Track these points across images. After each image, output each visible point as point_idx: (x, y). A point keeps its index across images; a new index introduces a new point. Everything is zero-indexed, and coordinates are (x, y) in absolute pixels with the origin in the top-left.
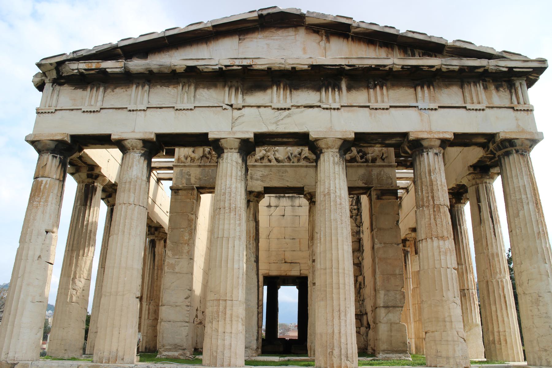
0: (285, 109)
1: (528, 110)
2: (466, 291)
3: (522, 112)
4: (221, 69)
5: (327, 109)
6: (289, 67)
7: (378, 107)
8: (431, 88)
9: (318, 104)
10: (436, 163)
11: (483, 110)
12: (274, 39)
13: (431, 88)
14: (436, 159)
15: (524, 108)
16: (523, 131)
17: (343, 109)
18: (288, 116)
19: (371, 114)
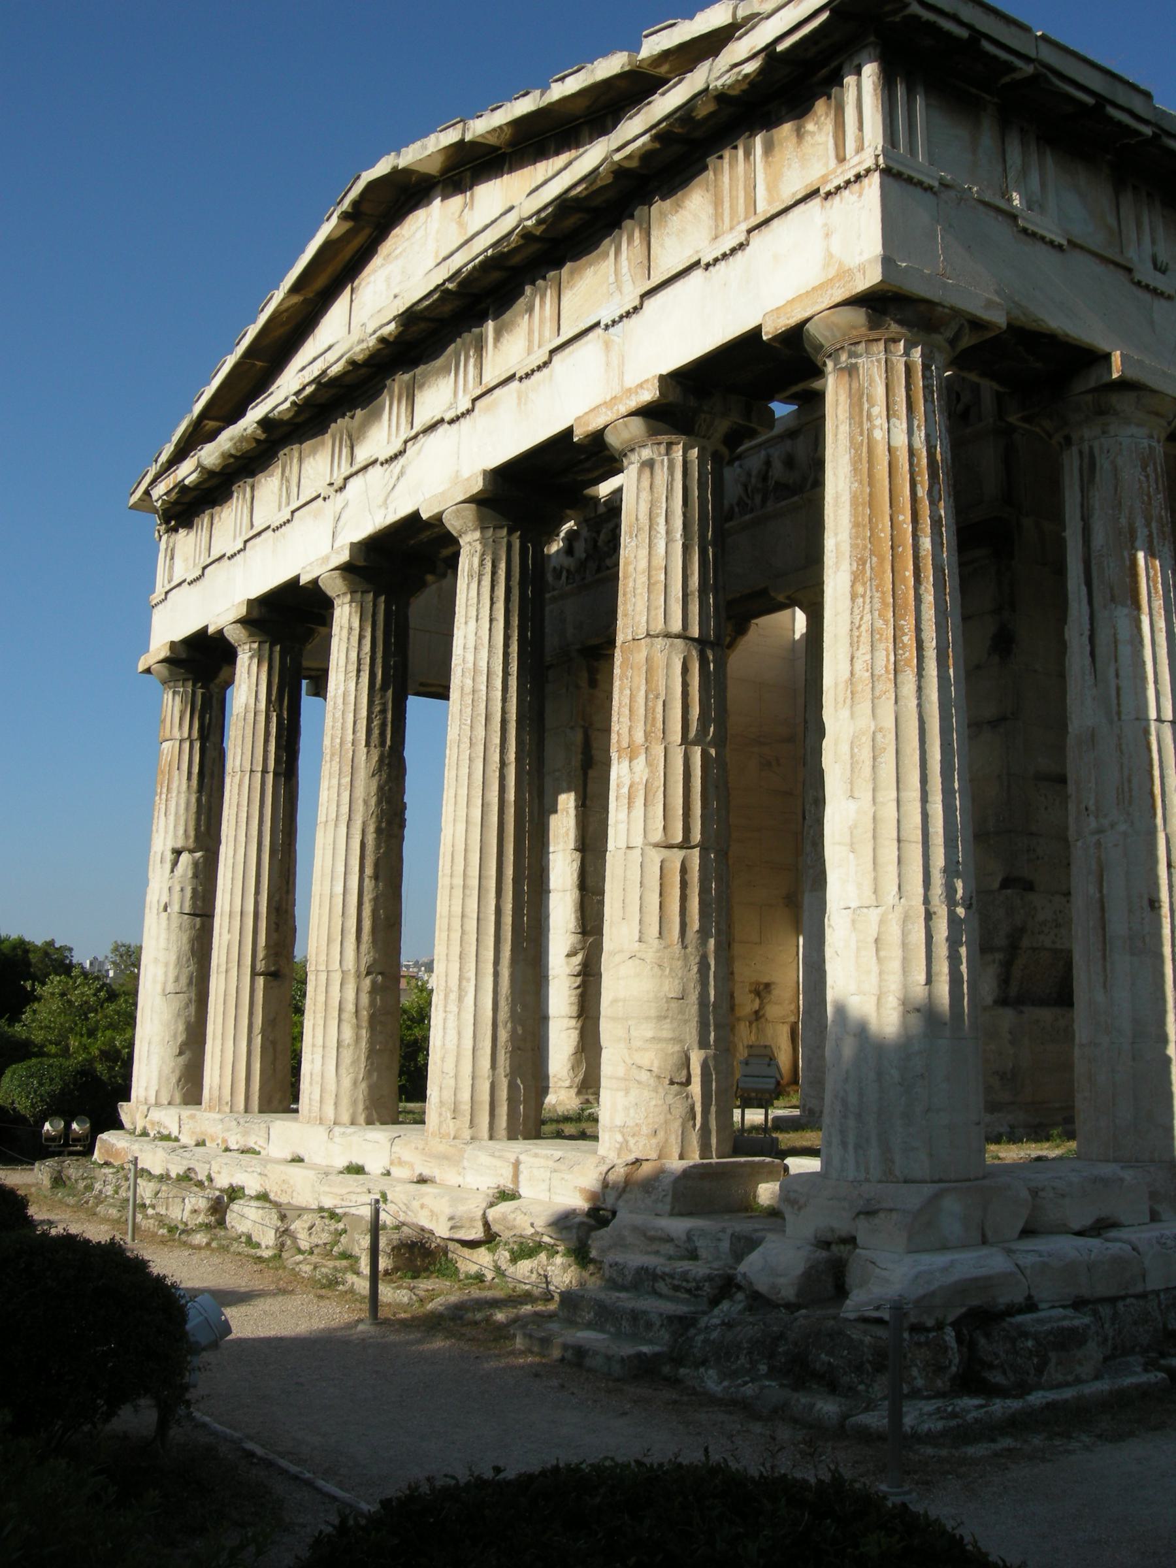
0: (395, 457)
1: (858, 177)
3: (846, 193)
4: (294, 403)
5: (452, 422)
6: (372, 342)
7: (528, 370)
8: (637, 234)
9: (438, 417)
10: (645, 495)
11: (741, 246)
12: (397, 258)
13: (637, 234)
14: (646, 483)
15: (846, 178)
16: (844, 274)
17: (478, 404)
18: (402, 473)
19: (519, 398)
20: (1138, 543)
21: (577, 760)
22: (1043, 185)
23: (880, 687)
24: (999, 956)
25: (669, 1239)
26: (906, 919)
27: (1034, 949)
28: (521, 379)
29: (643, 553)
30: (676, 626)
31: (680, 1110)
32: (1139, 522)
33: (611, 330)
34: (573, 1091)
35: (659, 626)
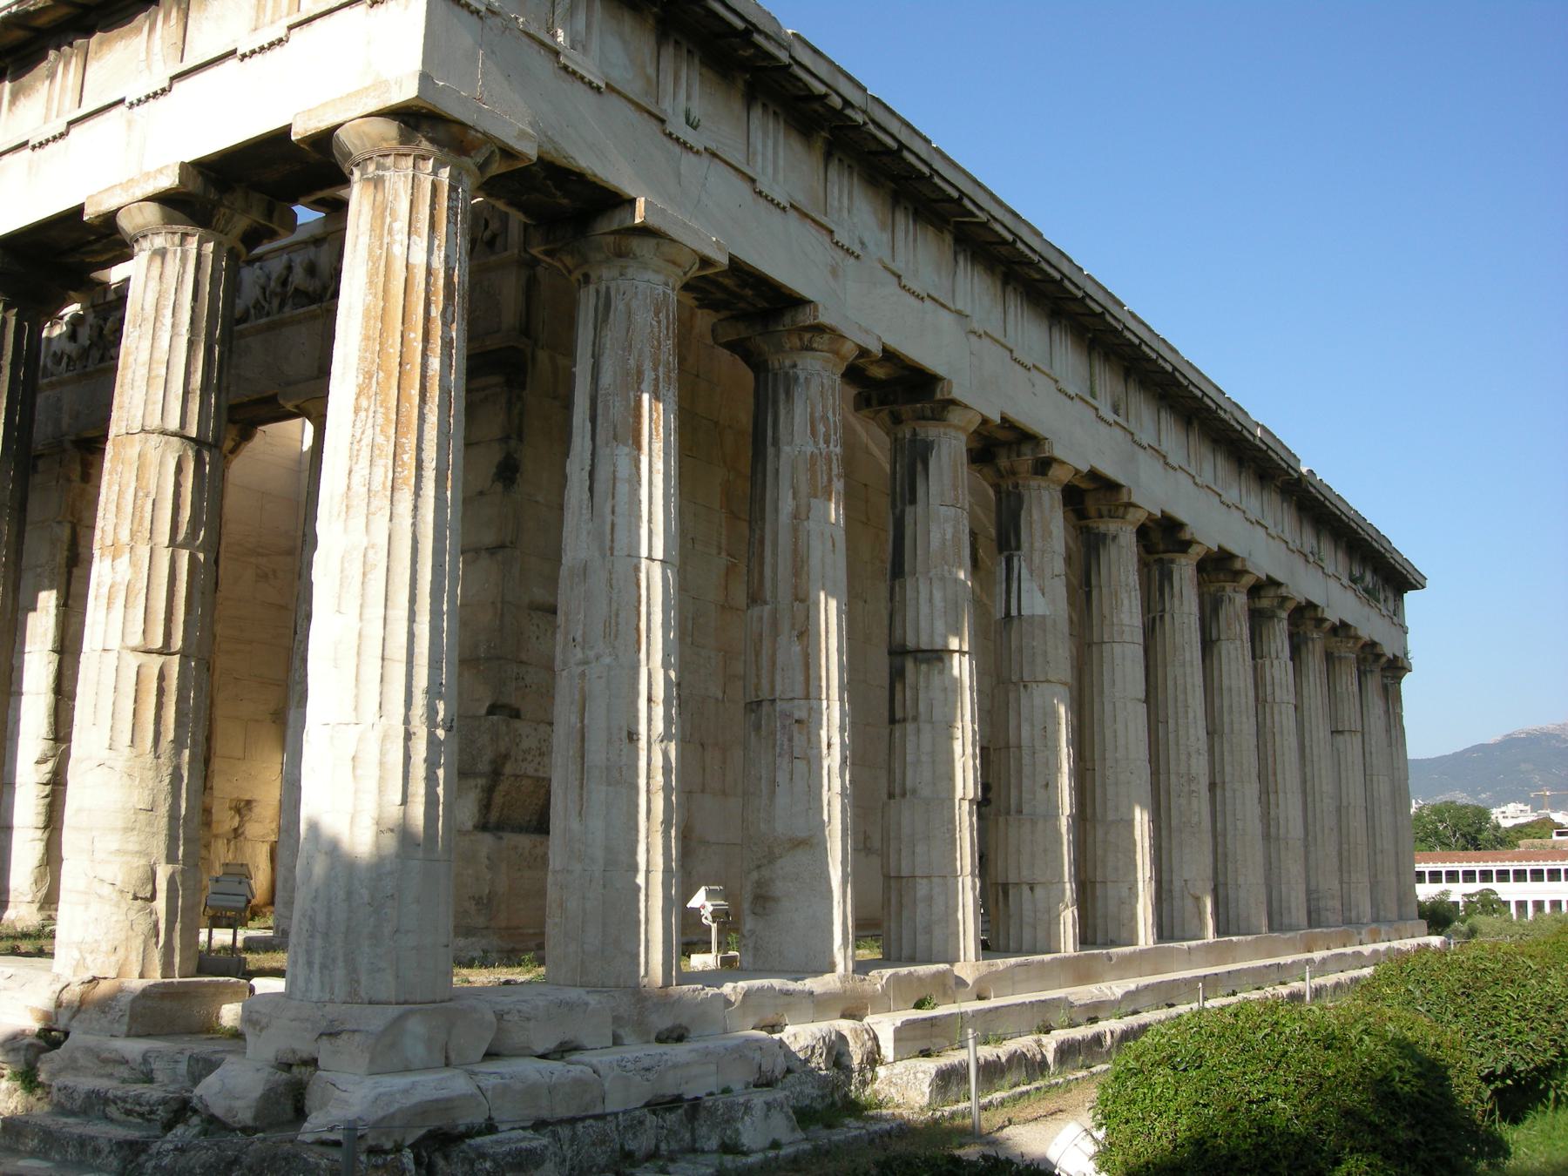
2: (766, 708)
8: (174, 13)
10: (154, 285)
13: (174, 13)
20: (644, 386)
21: (62, 556)
22: (588, 26)
23: (375, 503)
24: (481, 782)
25: (124, 1062)
26: (385, 738)
27: (517, 776)
28: (34, 147)
29: (146, 344)
30: (173, 423)
31: (143, 925)
32: (647, 365)
33: (136, 109)
34: (36, 906)
35: (154, 422)
